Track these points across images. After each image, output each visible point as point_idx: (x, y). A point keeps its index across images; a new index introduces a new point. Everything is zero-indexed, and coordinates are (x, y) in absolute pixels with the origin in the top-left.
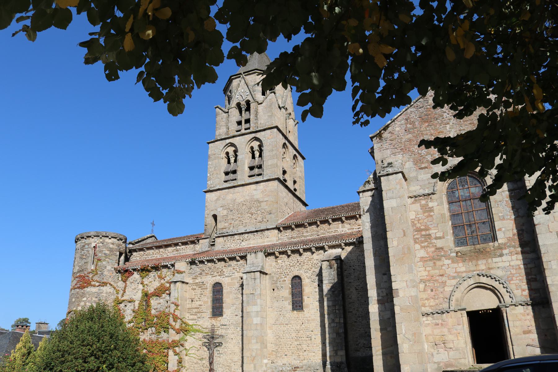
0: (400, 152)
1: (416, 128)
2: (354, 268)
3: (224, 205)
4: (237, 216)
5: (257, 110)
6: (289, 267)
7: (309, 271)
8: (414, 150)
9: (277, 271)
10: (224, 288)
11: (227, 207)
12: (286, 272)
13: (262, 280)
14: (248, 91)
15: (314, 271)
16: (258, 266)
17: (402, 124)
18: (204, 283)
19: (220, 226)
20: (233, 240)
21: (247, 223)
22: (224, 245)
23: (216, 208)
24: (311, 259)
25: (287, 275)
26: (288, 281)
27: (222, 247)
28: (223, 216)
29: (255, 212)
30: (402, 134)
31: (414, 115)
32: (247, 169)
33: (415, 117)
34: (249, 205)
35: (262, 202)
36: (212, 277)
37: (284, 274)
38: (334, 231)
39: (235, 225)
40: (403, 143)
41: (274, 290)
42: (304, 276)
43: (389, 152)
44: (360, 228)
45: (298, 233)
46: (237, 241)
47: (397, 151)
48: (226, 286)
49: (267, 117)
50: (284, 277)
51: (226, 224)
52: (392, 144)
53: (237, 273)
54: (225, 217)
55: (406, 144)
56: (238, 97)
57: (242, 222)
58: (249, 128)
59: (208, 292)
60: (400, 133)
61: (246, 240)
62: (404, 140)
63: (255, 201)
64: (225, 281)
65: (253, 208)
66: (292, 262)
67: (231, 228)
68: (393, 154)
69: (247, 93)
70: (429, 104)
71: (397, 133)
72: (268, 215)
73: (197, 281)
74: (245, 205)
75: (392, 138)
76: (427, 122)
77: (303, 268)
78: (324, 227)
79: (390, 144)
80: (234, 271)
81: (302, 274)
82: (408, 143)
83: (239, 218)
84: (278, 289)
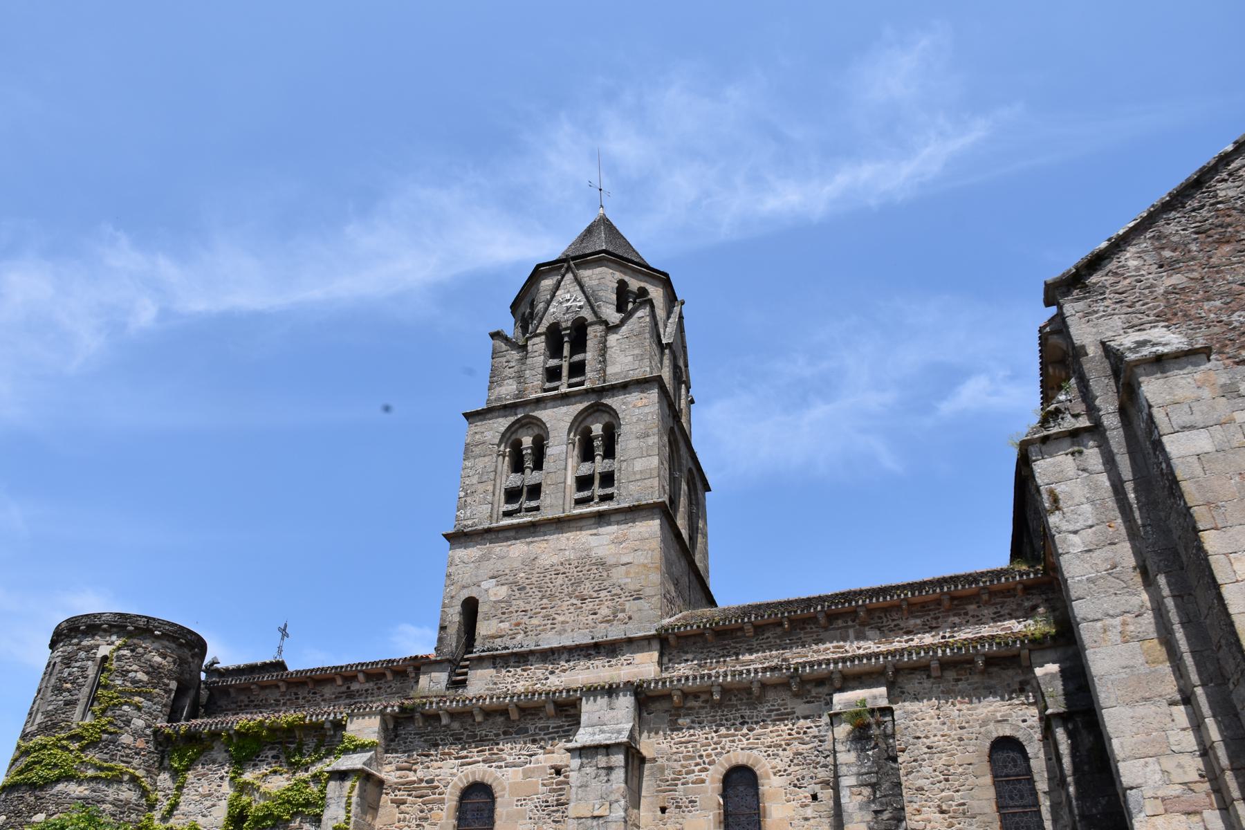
0: (1158, 321)
1: (1193, 259)
2: (928, 742)
3: (500, 573)
4: (538, 603)
5: (606, 340)
6: (715, 739)
7: (781, 753)
8: (1204, 315)
9: (675, 750)
10: (499, 800)
11: (511, 579)
12: (704, 753)
13: (630, 774)
14: (581, 297)
15: (801, 754)
16: (619, 732)
17: (1143, 251)
18: (436, 783)
19: (484, 628)
21: (568, 622)
22: (495, 684)
23: (475, 580)
24: (788, 714)
25: (710, 764)
26: (712, 782)
27: (488, 689)
28: (495, 602)
29: (591, 593)
30: (1150, 276)
31: (1179, 228)
32: (570, 481)
33: (1182, 232)
34: (575, 574)
35: (616, 565)
36: (462, 765)
37: (698, 760)
38: (834, 647)
39: (529, 628)
40: (1161, 298)
41: (663, 810)
42: (764, 765)
43: (1117, 322)
44: (912, 640)
45: (721, 653)
46: (535, 673)
47: (1146, 318)
48: (506, 796)
49: (630, 358)
50: (700, 771)
52: (1121, 301)
53: (544, 754)
54: (503, 605)
55: (1172, 301)
56: (555, 310)
57: (554, 619)
58: (582, 383)
59: (444, 814)
60: (1142, 272)
61: (564, 671)
62: (1161, 290)
63: (595, 564)
65: (587, 582)
66: (724, 722)
67: (519, 637)
68: (1132, 327)
69: (580, 301)
70: (1220, 199)
71: (1133, 273)
72: (632, 602)
73: (412, 777)
74: (564, 573)
75: (1120, 285)
76: (1228, 242)
77: (763, 743)
78: (802, 635)
79: (1117, 303)
81: (758, 761)
82: (1178, 296)
83: (542, 608)
84: (680, 807)
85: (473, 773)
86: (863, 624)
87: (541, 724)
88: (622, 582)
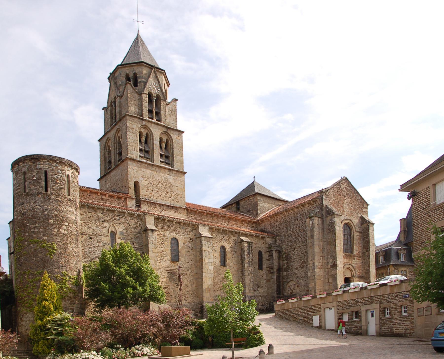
20: (155, 207)
51: (148, 193)
64: (180, 238)
80: (186, 233)
85: (173, 235)
86: (225, 219)
87: (187, 228)
88: (177, 191)
